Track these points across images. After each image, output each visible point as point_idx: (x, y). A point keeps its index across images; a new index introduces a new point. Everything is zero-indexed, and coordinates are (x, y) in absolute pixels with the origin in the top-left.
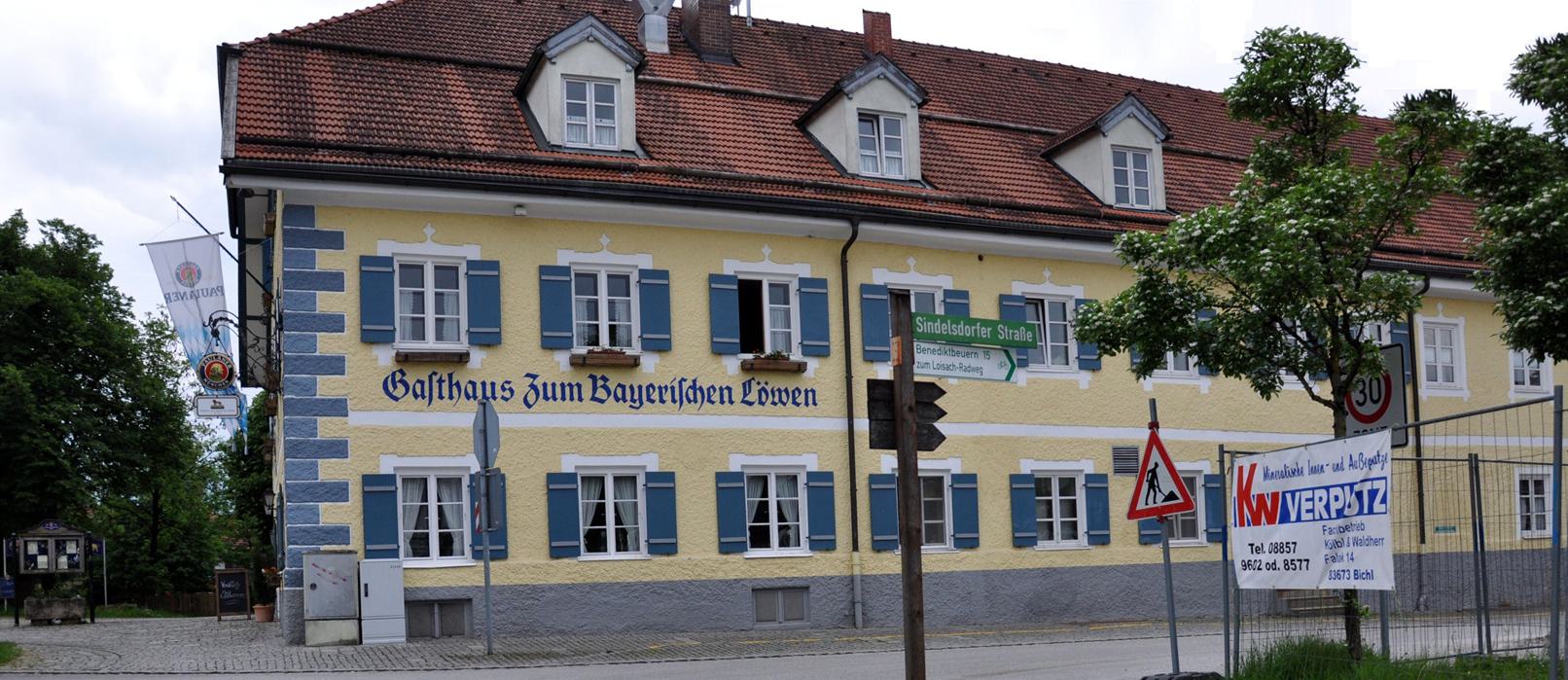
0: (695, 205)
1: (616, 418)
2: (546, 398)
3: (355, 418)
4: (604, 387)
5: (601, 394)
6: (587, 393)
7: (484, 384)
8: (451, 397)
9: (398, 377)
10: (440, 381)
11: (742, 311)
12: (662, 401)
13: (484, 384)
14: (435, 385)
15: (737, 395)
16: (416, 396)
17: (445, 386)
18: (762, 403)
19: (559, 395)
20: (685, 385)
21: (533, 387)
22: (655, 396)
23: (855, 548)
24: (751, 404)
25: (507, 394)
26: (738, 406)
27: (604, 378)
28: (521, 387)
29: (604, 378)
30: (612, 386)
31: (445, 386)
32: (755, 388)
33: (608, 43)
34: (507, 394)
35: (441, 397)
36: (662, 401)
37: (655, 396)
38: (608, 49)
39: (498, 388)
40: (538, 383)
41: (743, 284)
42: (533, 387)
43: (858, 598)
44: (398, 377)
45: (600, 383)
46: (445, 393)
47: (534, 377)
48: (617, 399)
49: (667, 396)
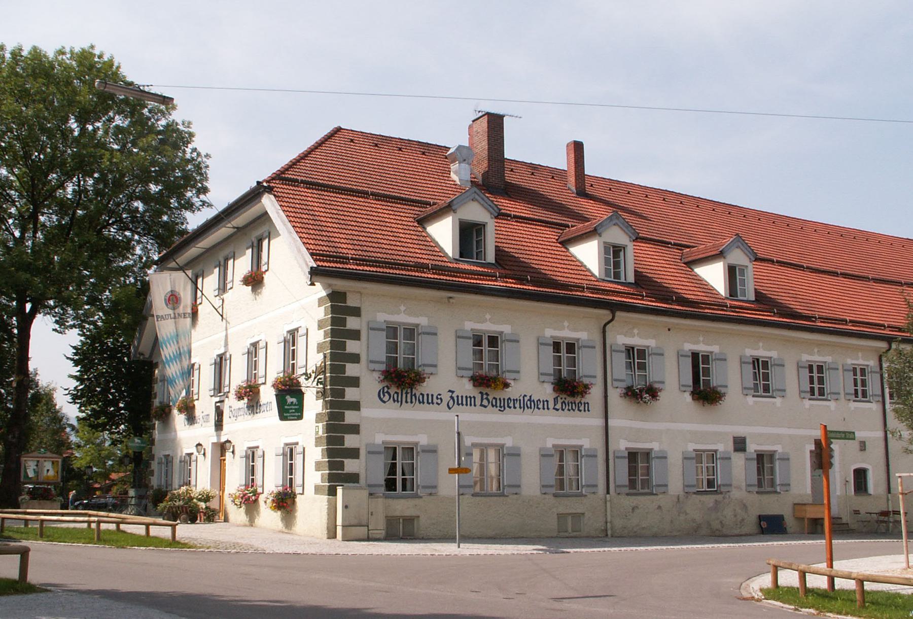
0: (439, 289)
1: (492, 416)
2: (458, 404)
3: (365, 412)
4: (487, 399)
5: (485, 402)
6: (478, 402)
7: (428, 395)
8: (412, 402)
9: (386, 390)
10: (407, 393)
11: (761, 367)
12: (515, 408)
13: (428, 395)
14: (404, 396)
15: (551, 405)
16: (394, 401)
17: (409, 396)
18: (563, 410)
19: (464, 403)
20: (526, 399)
21: (452, 397)
22: (511, 405)
23: (608, 492)
24: (557, 410)
25: (439, 401)
26: (551, 410)
27: (487, 394)
28: (446, 397)
29: (487, 394)
30: (490, 398)
31: (409, 396)
32: (560, 401)
33: (482, 202)
34: (439, 401)
35: (406, 402)
36: (515, 408)
37: (511, 405)
38: (482, 205)
39: (435, 397)
40: (454, 395)
41: (693, 353)
42: (452, 397)
43: (609, 520)
44: (386, 390)
45: (485, 396)
46: (409, 400)
47: (453, 392)
48: (493, 406)
49: (517, 405)
